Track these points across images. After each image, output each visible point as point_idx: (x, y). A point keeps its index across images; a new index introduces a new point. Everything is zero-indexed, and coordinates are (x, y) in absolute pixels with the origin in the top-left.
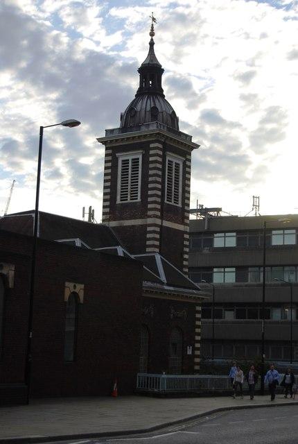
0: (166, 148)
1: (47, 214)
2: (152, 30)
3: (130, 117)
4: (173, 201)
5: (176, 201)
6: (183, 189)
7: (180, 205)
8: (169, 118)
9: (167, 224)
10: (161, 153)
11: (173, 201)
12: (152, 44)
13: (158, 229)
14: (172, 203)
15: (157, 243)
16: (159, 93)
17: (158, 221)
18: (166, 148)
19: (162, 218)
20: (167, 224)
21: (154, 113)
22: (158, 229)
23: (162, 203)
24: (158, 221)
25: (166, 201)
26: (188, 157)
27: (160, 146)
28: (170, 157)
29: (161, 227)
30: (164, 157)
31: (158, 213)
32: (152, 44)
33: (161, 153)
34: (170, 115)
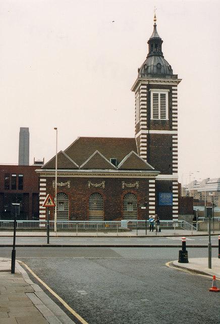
0: (149, 87)
1: (102, 138)
2: (155, 17)
3: (144, 70)
4: (159, 117)
5: (163, 115)
6: (170, 109)
7: (167, 119)
8: (155, 68)
9: (152, 132)
10: (145, 91)
11: (159, 117)
12: (155, 26)
13: (146, 136)
14: (159, 119)
15: (146, 144)
16: (160, 55)
17: (146, 132)
18: (149, 87)
19: (149, 129)
20: (152, 132)
21: (159, 67)
22: (146, 136)
23: (148, 120)
24: (146, 132)
25: (152, 118)
26: (173, 88)
27: (145, 87)
28: (153, 92)
29: (148, 135)
30: (149, 94)
31: (146, 127)
32: (155, 26)
33: (145, 91)
34: (157, 66)
